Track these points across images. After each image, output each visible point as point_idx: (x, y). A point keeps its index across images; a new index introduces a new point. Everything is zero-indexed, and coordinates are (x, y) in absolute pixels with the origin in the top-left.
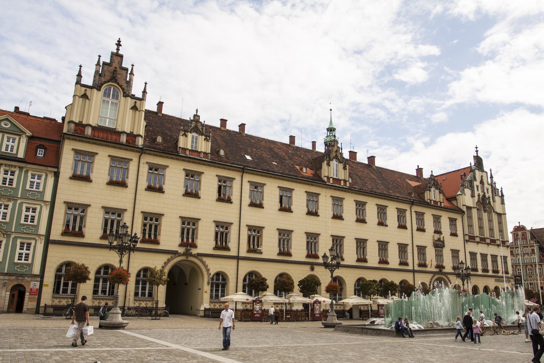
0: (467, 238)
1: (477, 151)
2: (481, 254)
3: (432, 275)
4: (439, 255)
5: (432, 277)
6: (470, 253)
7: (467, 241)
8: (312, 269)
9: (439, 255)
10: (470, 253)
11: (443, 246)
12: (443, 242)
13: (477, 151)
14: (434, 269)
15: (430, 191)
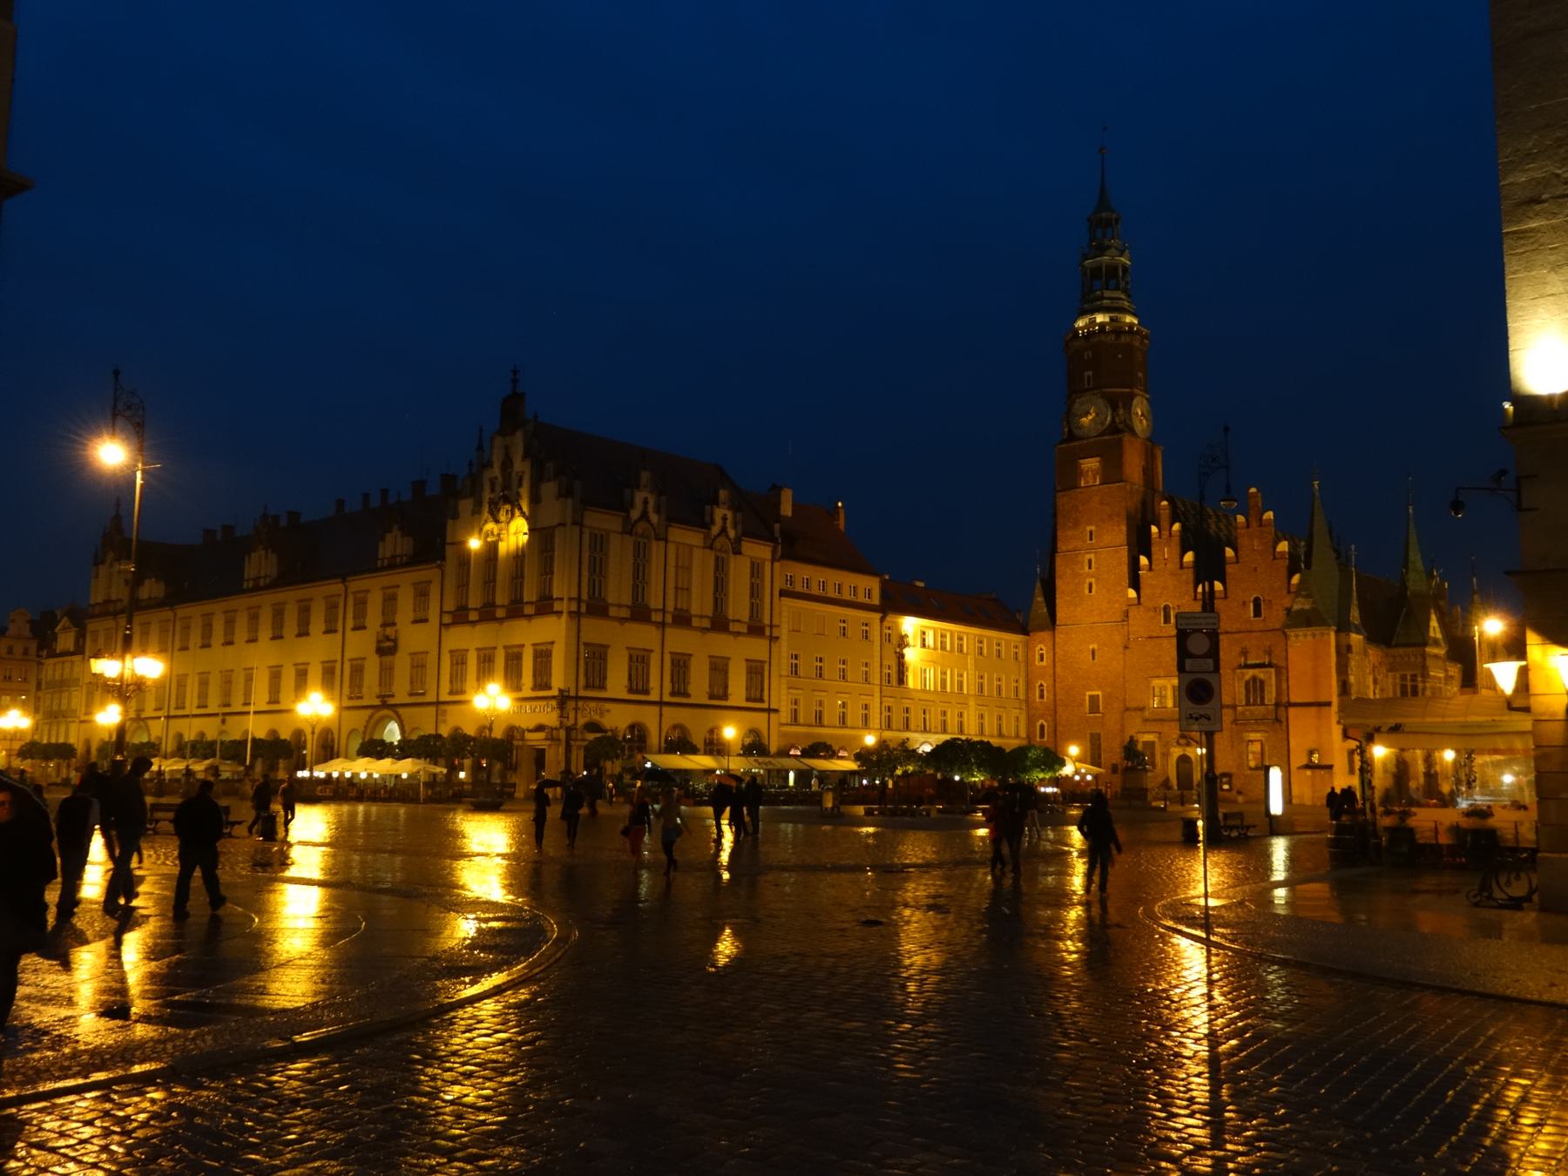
0: (447, 619)
1: (515, 381)
2: (478, 649)
3: (369, 712)
4: (386, 673)
5: (371, 717)
6: (451, 652)
7: (447, 625)
8: (223, 721)
9: (386, 673)
10: (451, 652)
11: (392, 651)
12: (395, 641)
13: (515, 381)
14: (377, 702)
15: (383, 539)
